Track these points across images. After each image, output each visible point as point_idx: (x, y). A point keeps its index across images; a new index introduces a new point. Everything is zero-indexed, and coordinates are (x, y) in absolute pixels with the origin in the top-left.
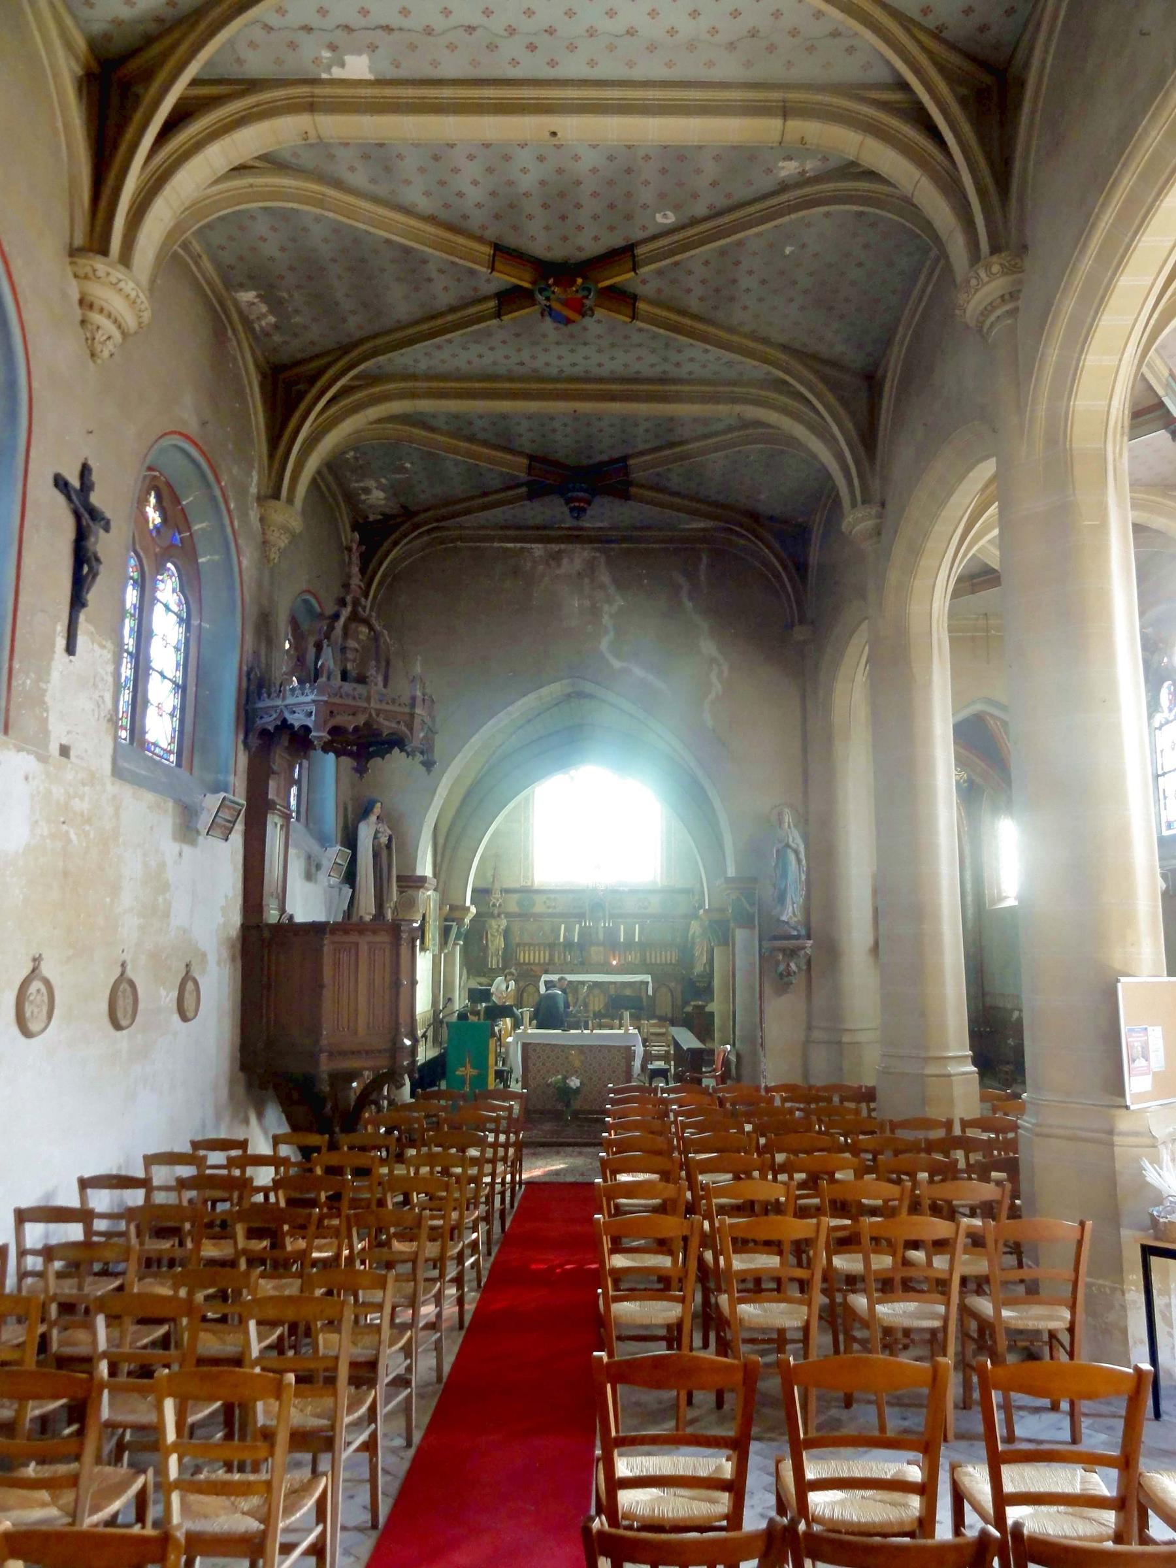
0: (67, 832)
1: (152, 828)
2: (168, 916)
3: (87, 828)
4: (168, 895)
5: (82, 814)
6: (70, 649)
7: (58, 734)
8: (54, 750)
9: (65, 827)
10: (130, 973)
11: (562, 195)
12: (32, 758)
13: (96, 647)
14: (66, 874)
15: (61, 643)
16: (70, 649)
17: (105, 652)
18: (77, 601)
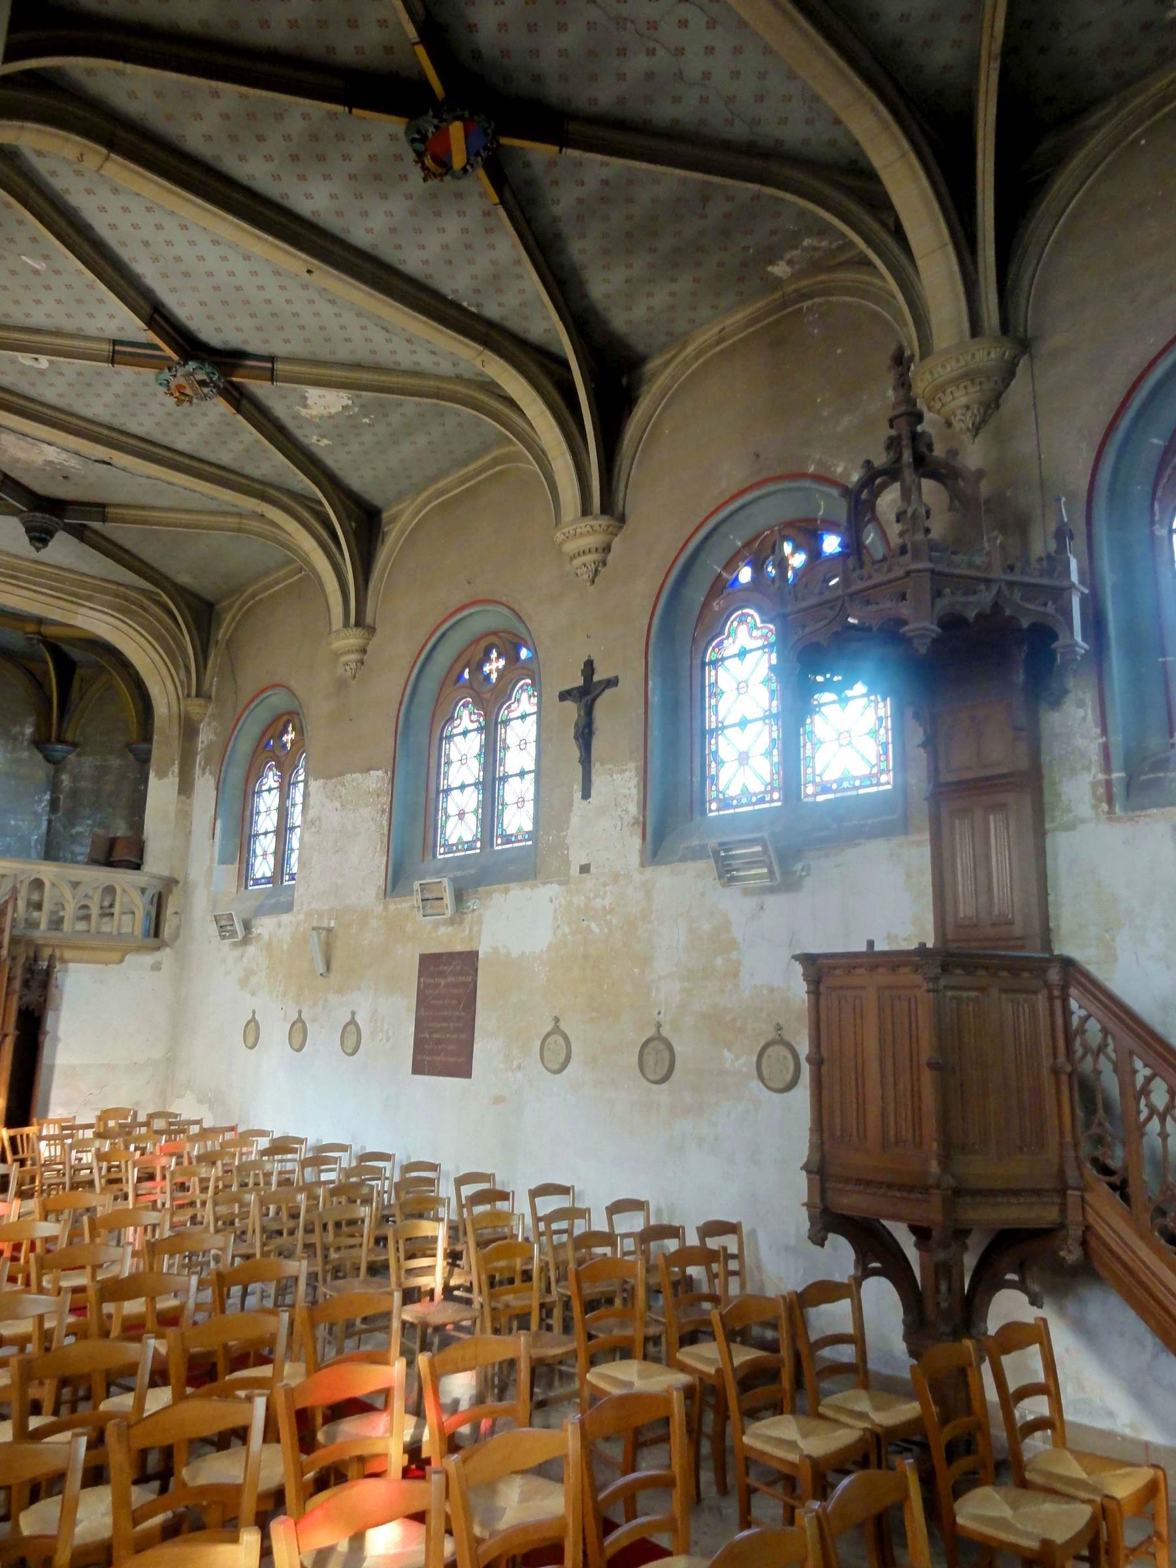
0: (588, 927)
1: (703, 895)
2: (736, 975)
3: (609, 917)
4: (734, 955)
5: (604, 908)
6: (586, 794)
7: (577, 857)
8: (574, 870)
9: (585, 923)
10: (666, 1032)
11: (377, 177)
12: (555, 886)
13: (615, 776)
14: (586, 957)
15: (578, 795)
16: (586, 794)
17: (627, 774)
18: (586, 761)
